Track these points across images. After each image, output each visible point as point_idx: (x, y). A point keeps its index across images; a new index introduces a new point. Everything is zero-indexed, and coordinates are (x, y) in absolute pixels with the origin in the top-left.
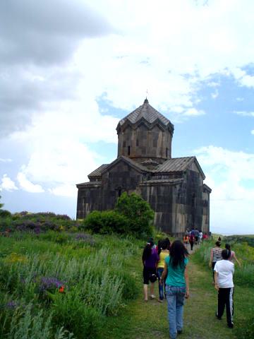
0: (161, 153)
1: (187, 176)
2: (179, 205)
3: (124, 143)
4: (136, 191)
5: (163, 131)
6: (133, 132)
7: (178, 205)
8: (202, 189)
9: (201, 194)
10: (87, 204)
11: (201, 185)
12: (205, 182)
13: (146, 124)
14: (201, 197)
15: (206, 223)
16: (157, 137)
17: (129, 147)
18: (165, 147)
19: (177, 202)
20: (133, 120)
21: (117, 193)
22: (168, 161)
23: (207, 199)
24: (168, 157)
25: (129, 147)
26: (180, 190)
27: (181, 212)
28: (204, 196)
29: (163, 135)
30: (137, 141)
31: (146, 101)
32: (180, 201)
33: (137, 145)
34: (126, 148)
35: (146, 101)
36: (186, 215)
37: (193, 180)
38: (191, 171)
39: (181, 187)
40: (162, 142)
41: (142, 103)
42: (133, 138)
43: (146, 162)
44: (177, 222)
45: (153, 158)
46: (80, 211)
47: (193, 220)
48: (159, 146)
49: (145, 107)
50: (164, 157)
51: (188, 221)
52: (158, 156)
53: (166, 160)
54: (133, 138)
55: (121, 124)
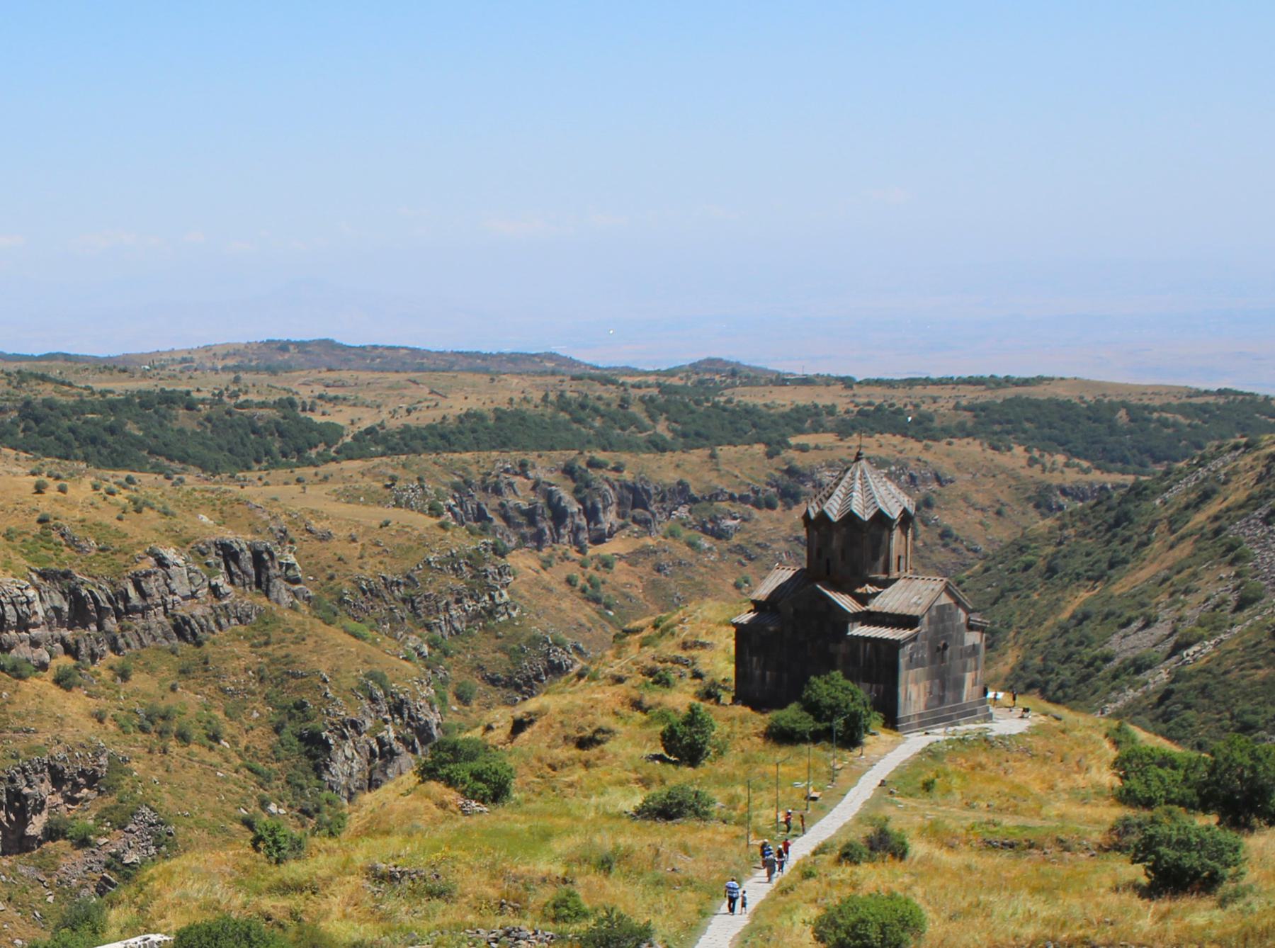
1: (930, 619)
2: (912, 673)
8: (964, 628)
14: (962, 642)
15: (974, 684)
17: (828, 562)
19: (909, 667)
20: (834, 516)
22: (900, 582)
24: (903, 570)
25: (828, 562)
27: (916, 682)
32: (913, 663)
36: (928, 683)
37: (942, 620)
38: (938, 607)
42: (836, 543)
43: (859, 591)
44: (908, 698)
45: (873, 582)
47: (943, 687)
50: (894, 575)
51: (931, 693)
53: (895, 580)
54: (836, 543)
55: (813, 516)
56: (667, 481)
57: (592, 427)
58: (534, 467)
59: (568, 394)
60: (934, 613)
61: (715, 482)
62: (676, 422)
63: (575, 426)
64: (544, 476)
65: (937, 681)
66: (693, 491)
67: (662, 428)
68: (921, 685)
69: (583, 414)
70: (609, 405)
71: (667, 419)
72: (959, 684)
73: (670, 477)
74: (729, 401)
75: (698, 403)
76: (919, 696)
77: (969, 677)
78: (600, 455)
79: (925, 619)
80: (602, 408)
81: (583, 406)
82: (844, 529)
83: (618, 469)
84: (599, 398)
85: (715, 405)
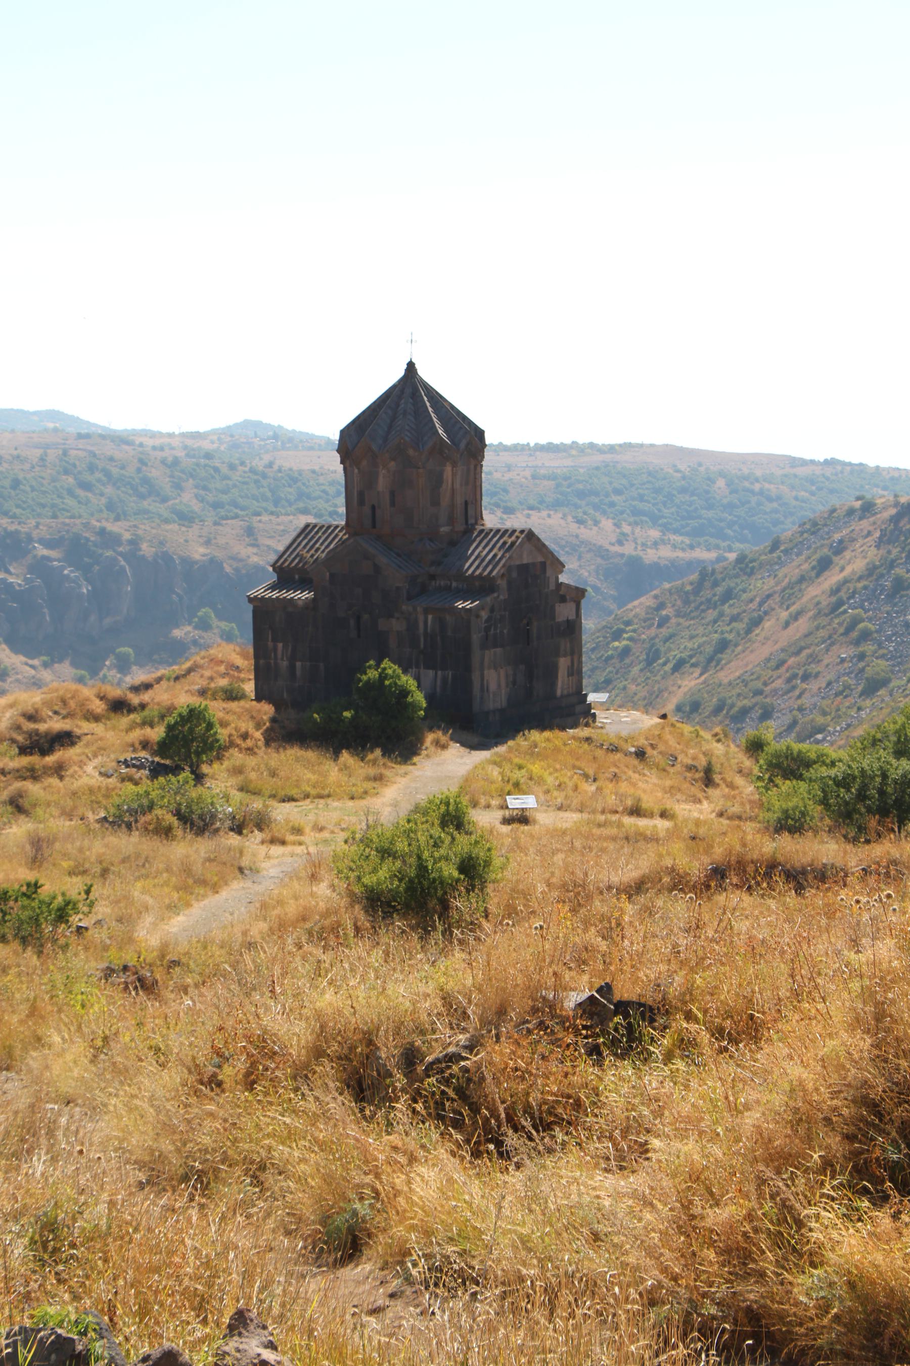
0: (451, 520)
1: (509, 583)
2: (489, 654)
3: (361, 494)
4: (394, 621)
5: (454, 465)
6: (382, 472)
7: (487, 652)
9: (553, 607)
10: (280, 645)
11: (552, 586)
12: (563, 578)
13: (411, 452)
14: (553, 617)
16: (437, 481)
18: (459, 500)
19: (484, 646)
21: (352, 622)
23: (572, 617)
25: (373, 508)
26: (487, 621)
28: (564, 612)
29: (454, 475)
30: (392, 494)
31: (411, 366)
33: (393, 504)
34: (367, 509)
35: (411, 366)
39: (492, 610)
40: (453, 490)
41: (400, 373)
42: (382, 483)
44: (484, 689)
46: (262, 662)
48: (445, 501)
49: (408, 391)
51: (514, 683)
52: (444, 529)
56: (197, 557)
57: (102, 495)
58: (30, 539)
59: (73, 453)
60: (514, 575)
61: (255, 559)
62: (205, 488)
63: (81, 493)
64: (42, 551)
65: (522, 667)
66: (228, 569)
67: (188, 499)
68: (502, 672)
69: (88, 477)
70: (123, 468)
71: (197, 487)
72: (551, 673)
73: (199, 552)
74: (270, 465)
75: (232, 467)
76: (499, 686)
77: (563, 663)
78: (113, 527)
79: (502, 583)
80: (115, 471)
81: (92, 468)
82: (393, 464)
83: (134, 543)
84: (111, 459)
85: (253, 471)
